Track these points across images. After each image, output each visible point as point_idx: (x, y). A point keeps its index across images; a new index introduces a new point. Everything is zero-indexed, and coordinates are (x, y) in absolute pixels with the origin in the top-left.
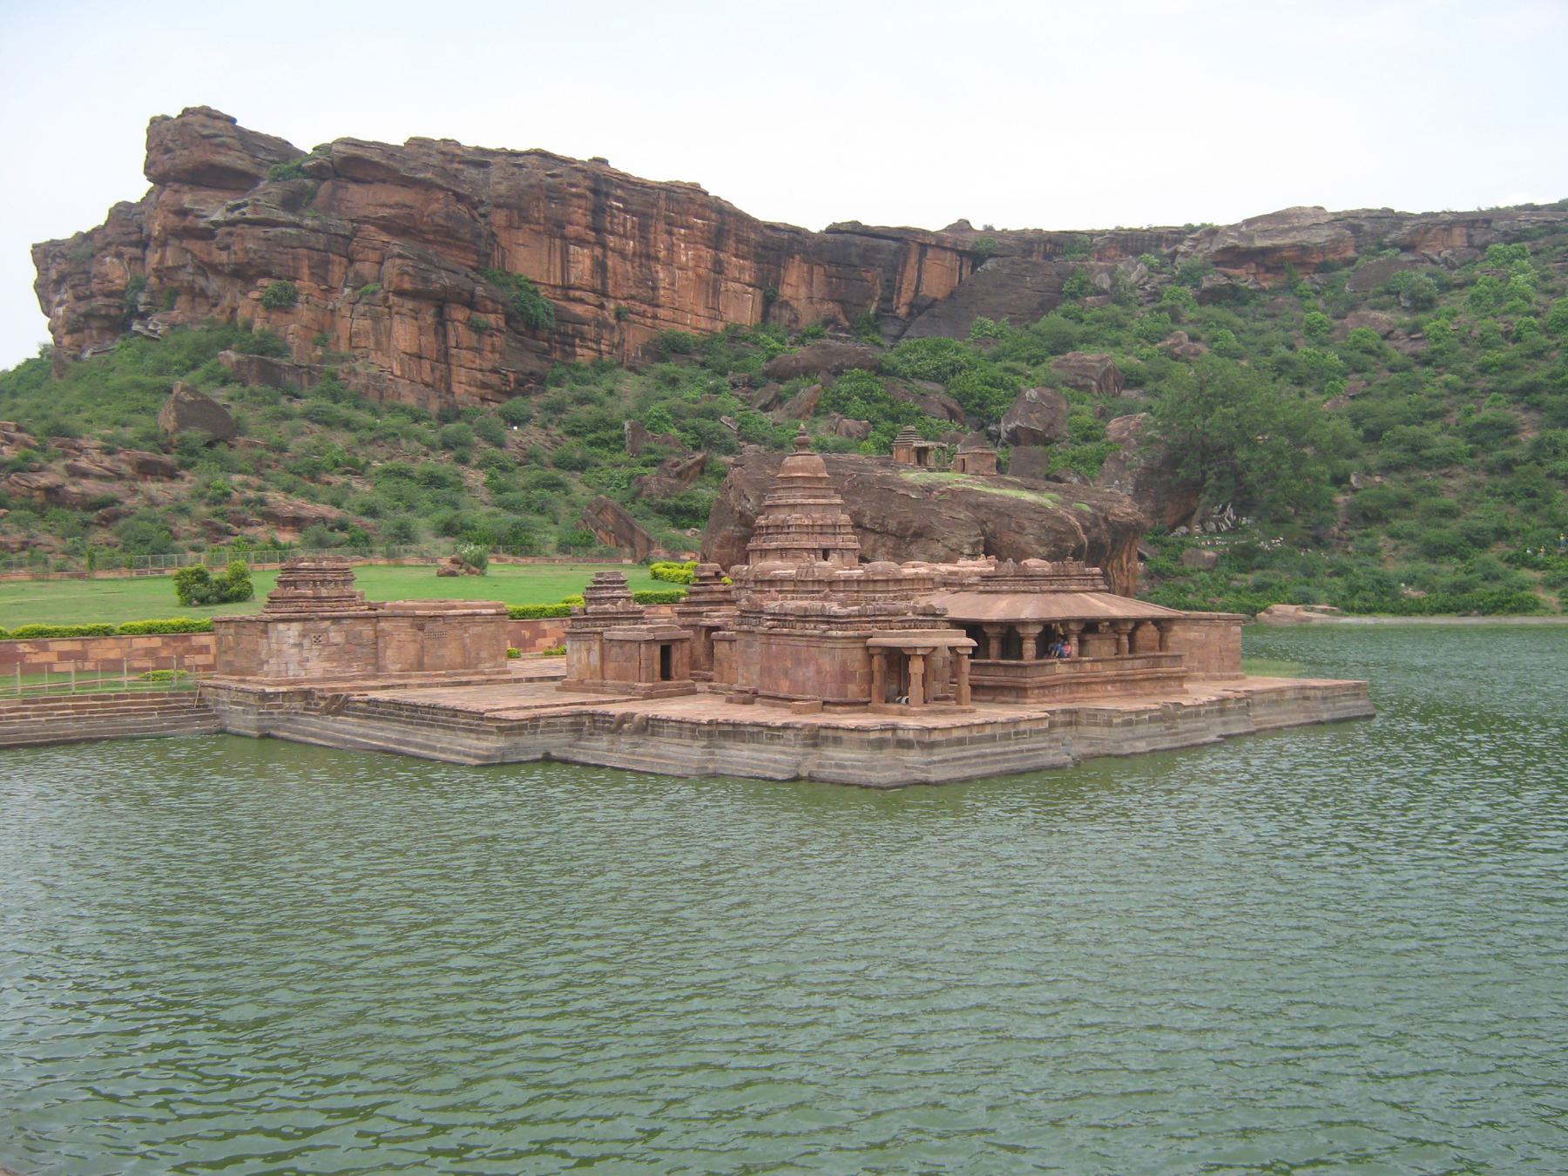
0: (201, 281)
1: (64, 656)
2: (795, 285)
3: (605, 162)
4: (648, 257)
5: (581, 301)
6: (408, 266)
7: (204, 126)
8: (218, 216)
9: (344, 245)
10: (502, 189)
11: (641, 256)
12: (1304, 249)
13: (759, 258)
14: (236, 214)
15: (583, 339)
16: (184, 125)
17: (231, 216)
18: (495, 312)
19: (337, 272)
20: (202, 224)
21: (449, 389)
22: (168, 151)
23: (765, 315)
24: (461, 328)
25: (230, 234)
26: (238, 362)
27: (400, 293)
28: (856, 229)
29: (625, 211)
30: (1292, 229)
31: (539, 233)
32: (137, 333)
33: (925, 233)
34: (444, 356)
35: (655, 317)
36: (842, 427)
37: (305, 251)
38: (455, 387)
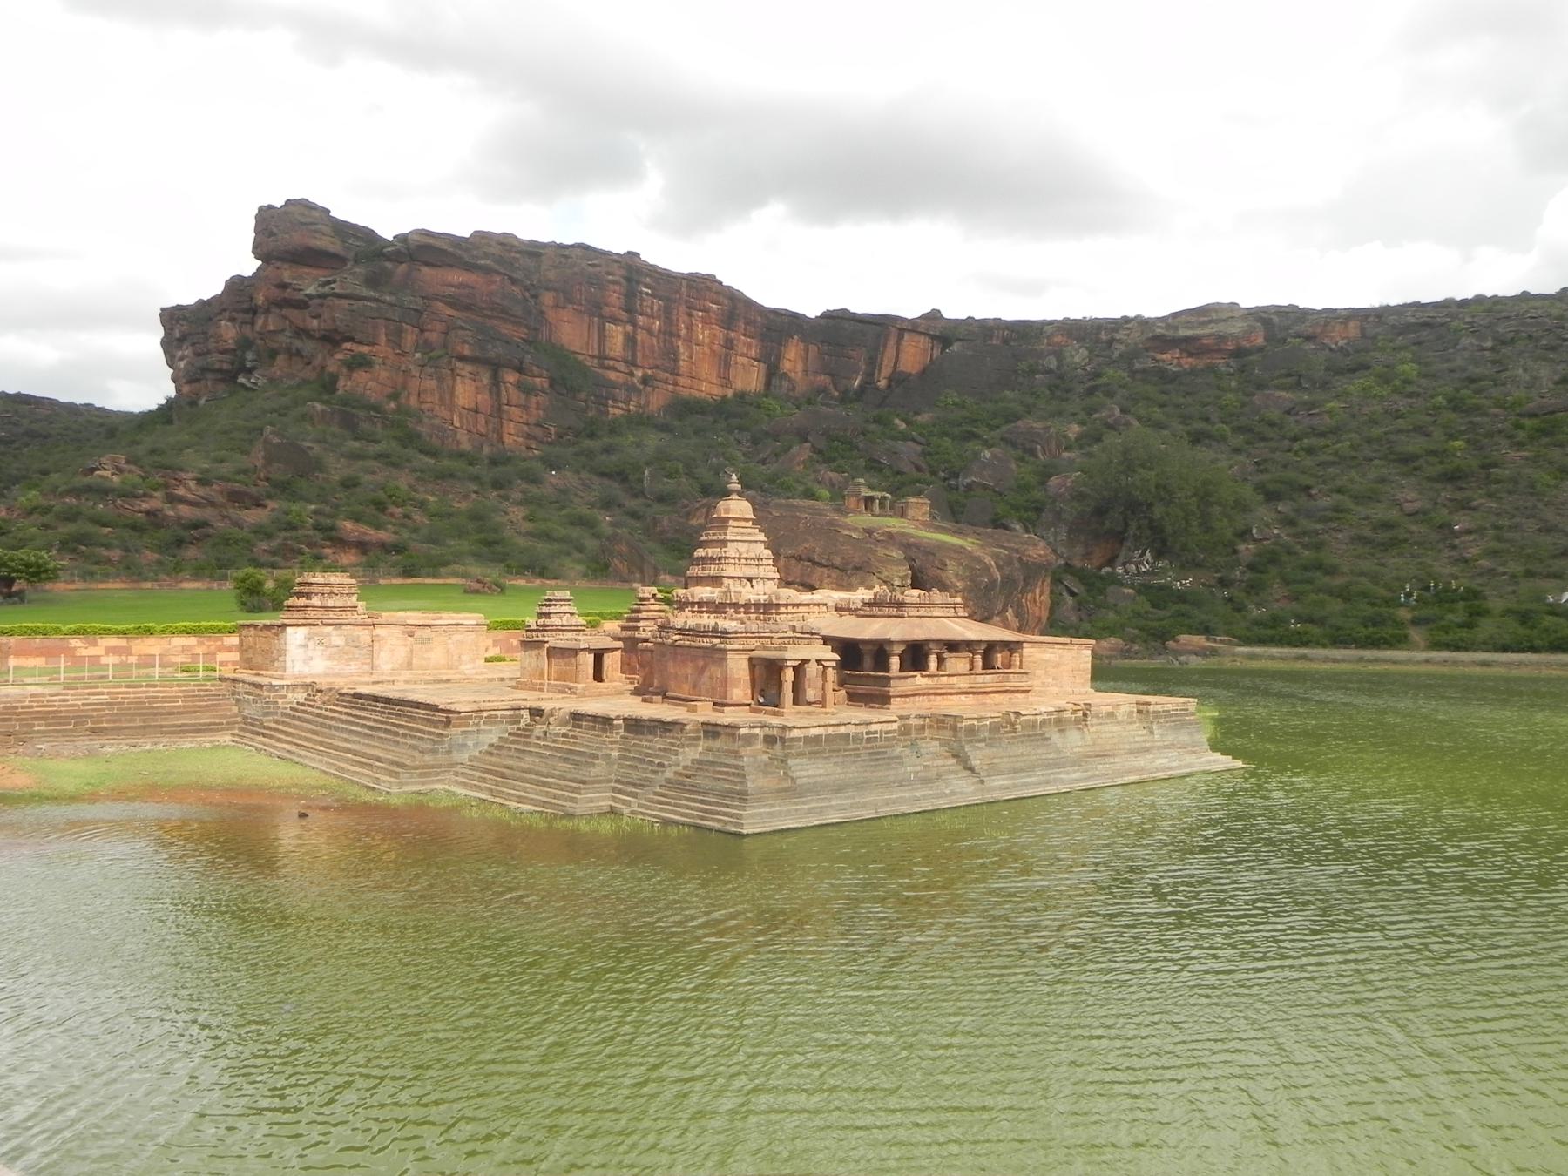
0: (298, 344)
1: (110, 650)
2: (792, 359)
4: (670, 333)
5: (614, 369)
7: (303, 215)
8: (310, 290)
12: (1221, 338)
14: (327, 289)
15: (615, 400)
19: (410, 337)
20: (300, 296)
22: (272, 234)
23: (768, 384)
24: (511, 388)
25: (322, 305)
27: (462, 358)
30: (1211, 321)
32: (242, 385)
34: (498, 412)
35: (676, 384)
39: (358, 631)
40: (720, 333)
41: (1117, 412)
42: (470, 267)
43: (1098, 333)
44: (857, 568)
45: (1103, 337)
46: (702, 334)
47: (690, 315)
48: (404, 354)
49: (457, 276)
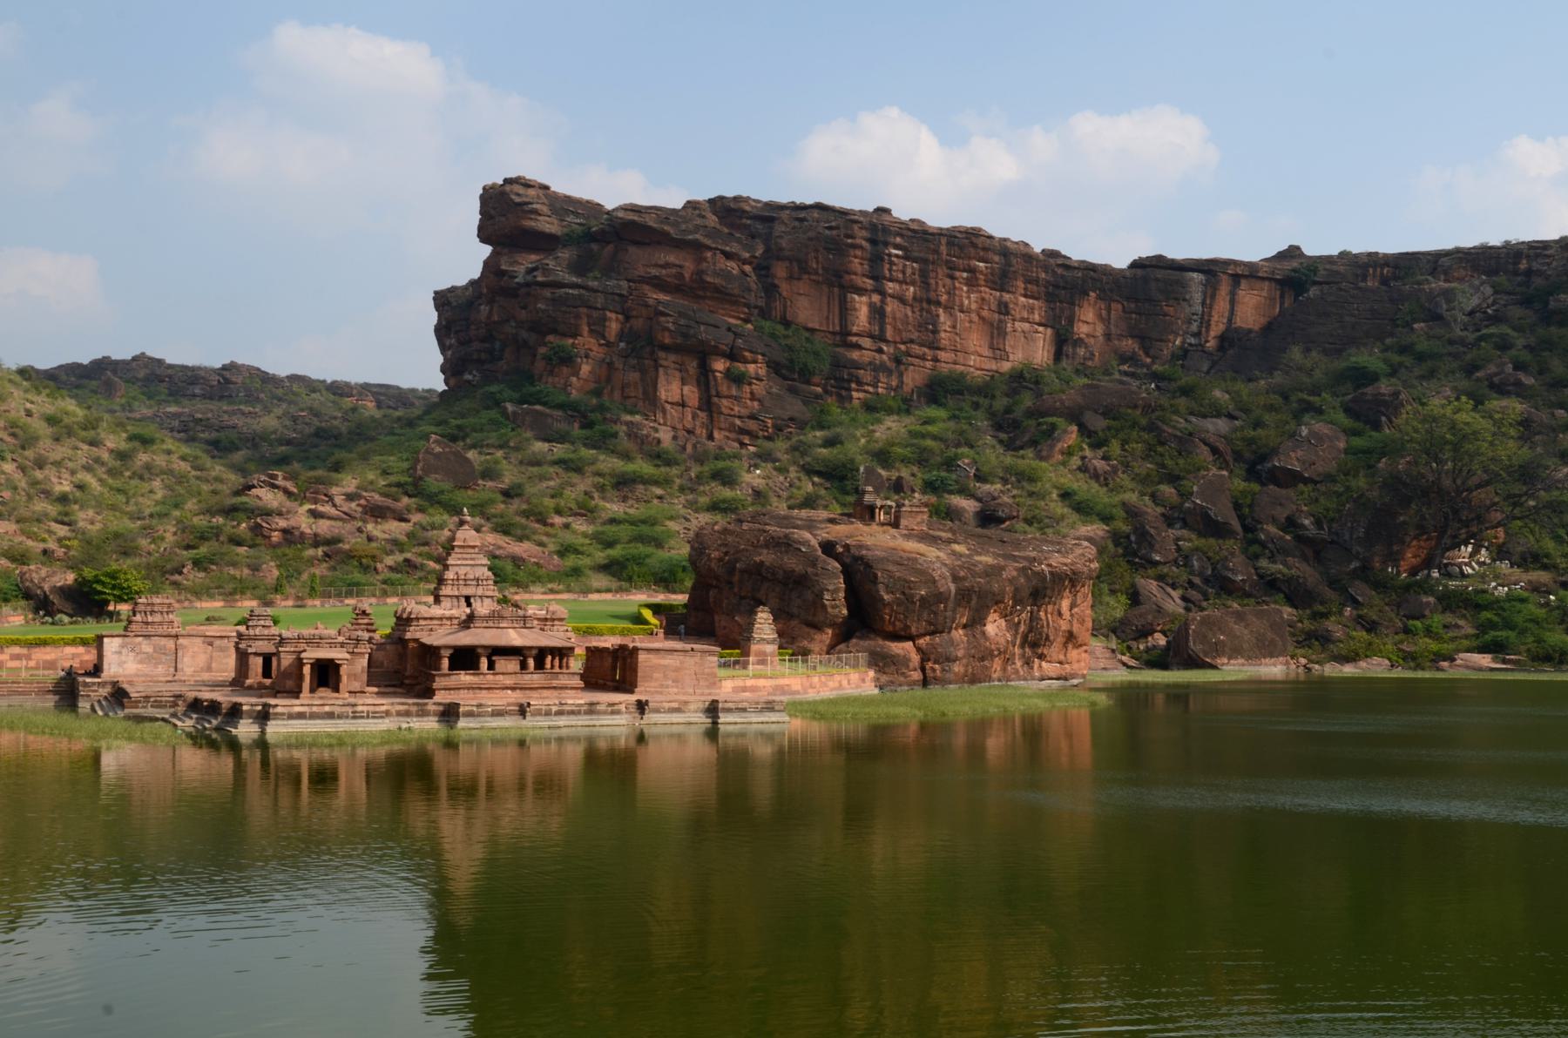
2: (1088, 322)
3: (886, 211)
4: (927, 301)
5: (858, 347)
10: (784, 243)
11: (921, 301)
13: (1050, 298)
15: (859, 383)
17: (529, 278)
18: (755, 362)
19: (614, 326)
22: (492, 217)
23: (1058, 355)
26: (514, 413)
29: (906, 258)
31: (817, 282)
35: (935, 360)
37: (583, 310)
38: (716, 434)
39: (163, 641)
40: (992, 295)
41: (1509, 368)
42: (679, 244)
43: (1516, 263)
45: (1523, 265)
46: (970, 299)
47: (952, 278)
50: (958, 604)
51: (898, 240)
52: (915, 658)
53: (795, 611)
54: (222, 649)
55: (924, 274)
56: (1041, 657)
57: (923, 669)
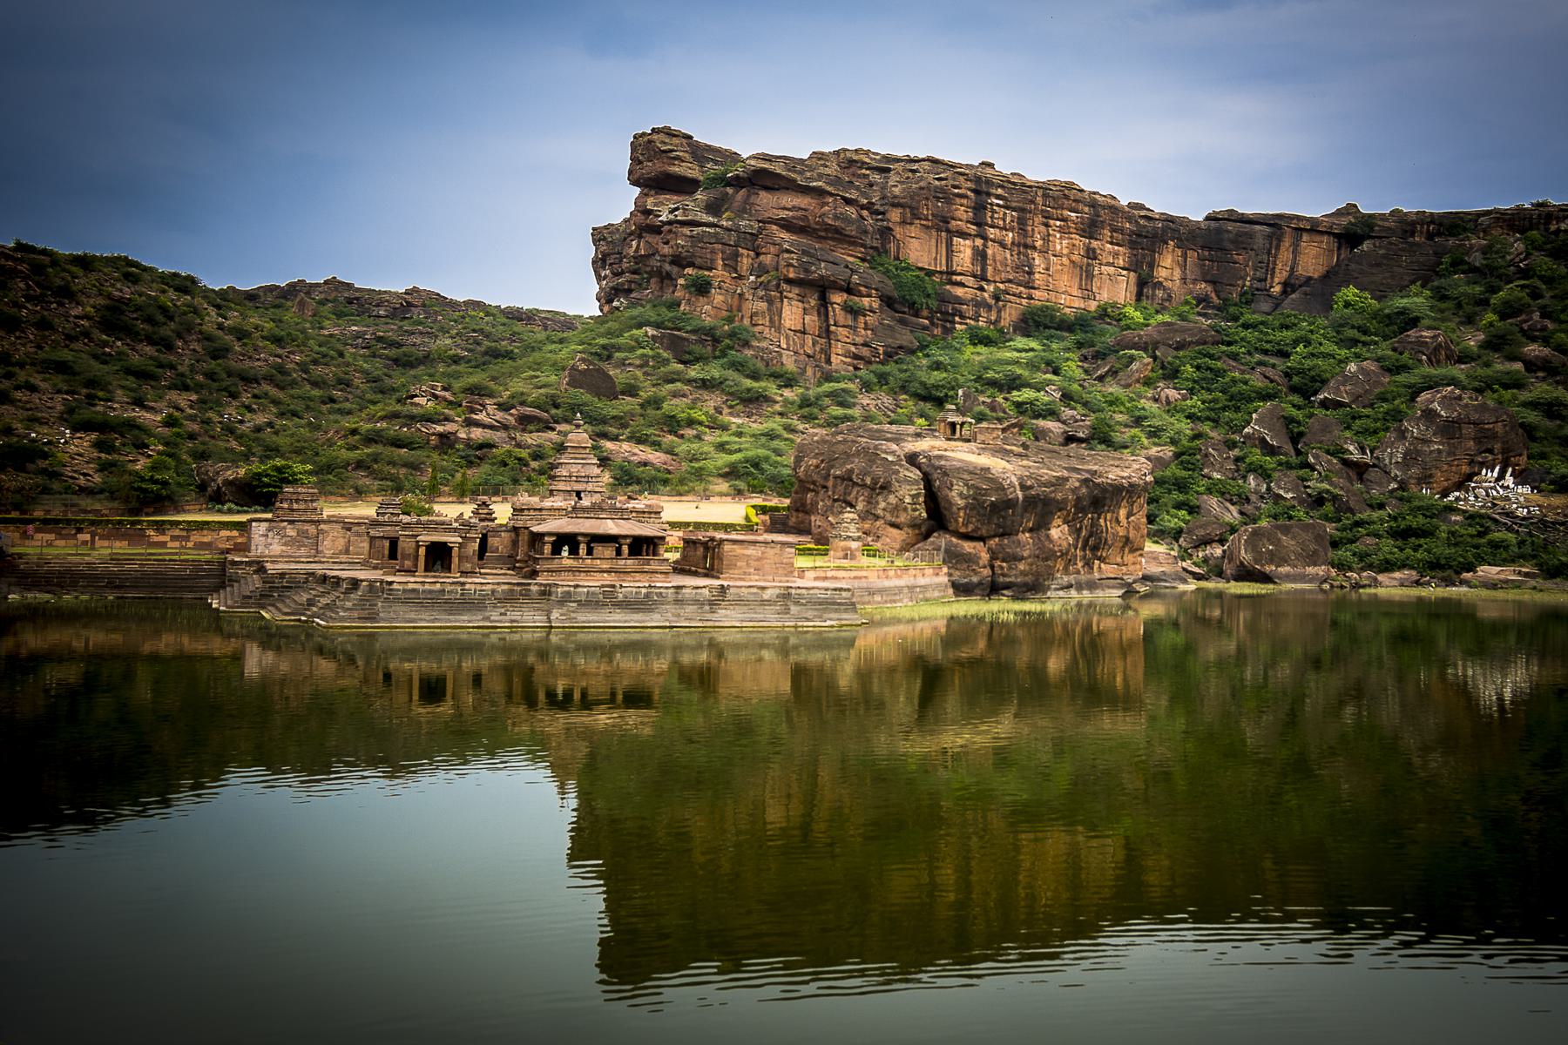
2: (1168, 267)
3: (991, 165)
4: (1024, 246)
6: (794, 259)
9: (753, 242)
10: (896, 191)
11: (1019, 245)
13: (1132, 245)
15: (962, 317)
16: (650, 142)
17: (671, 217)
18: (869, 296)
19: (745, 262)
21: (829, 361)
22: (640, 162)
23: (1139, 296)
27: (789, 281)
28: (1232, 217)
29: (1007, 208)
33: (1299, 218)
34: (826, 333)
35: (1030, 298)
36: (1163, 395)
40: (1080, 241)
41: (1536, 316)
44: (882, 488)
46: (1060, 244)
48: (740, 277)
49: (789, 200)
50: (1025, 510)
51: (1000, 191)
52: (985, 557)
53: (880, 512)
54: (358, 535)
55: (1022, 222)
56: (1102, 560)
57: (992, 567)
